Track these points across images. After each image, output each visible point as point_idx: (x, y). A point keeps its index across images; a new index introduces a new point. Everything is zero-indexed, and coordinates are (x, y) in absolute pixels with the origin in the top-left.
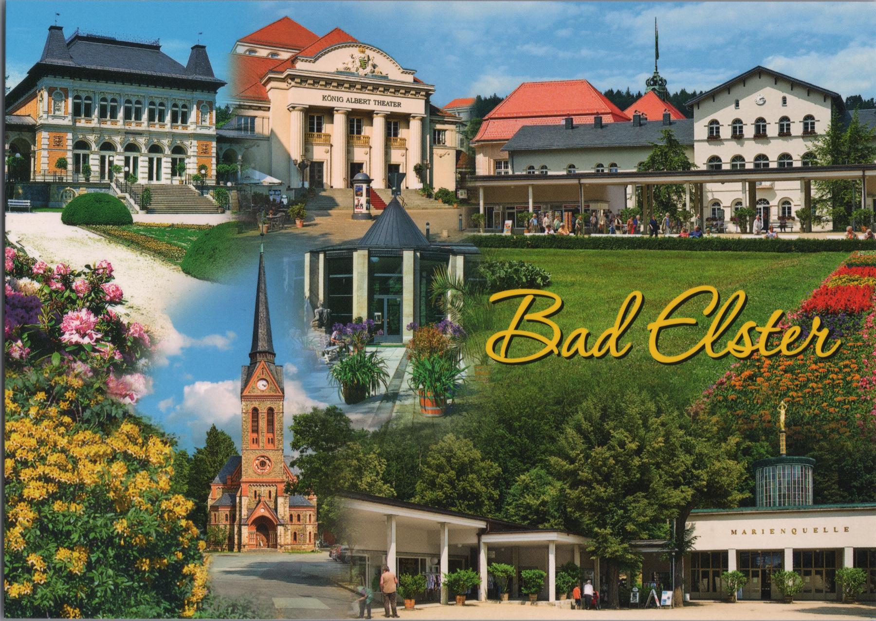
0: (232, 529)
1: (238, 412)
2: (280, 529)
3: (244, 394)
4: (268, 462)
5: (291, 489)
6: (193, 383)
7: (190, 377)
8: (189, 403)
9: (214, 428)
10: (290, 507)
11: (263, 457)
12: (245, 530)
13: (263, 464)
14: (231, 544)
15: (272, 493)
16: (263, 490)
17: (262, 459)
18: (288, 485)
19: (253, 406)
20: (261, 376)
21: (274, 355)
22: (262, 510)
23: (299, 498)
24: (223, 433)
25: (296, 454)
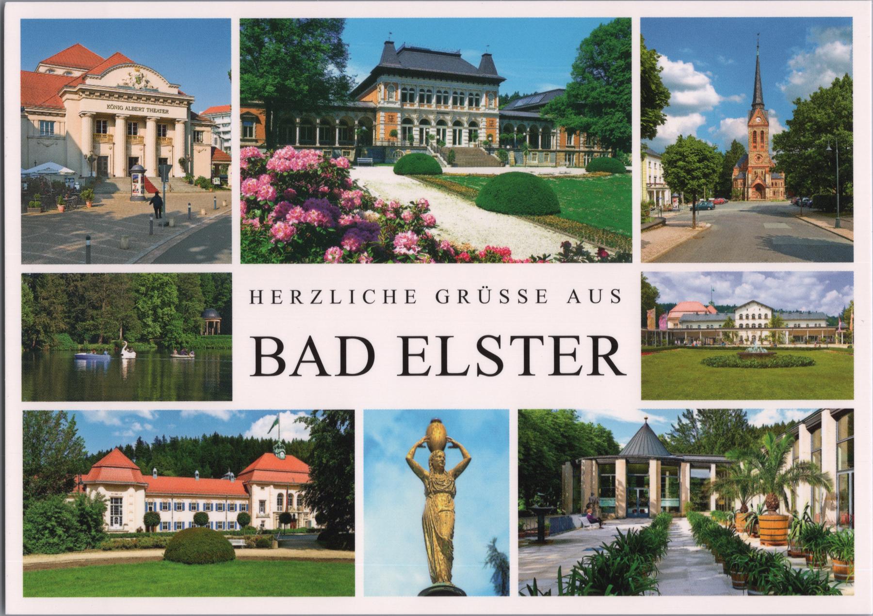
0: (744, 190)
1: (747, 133)
2: (767, 190)
3: (750, 124)
5: (772, 170)
6: (724, 119)
7: (723, 116)
8: (723, 129)
9: (735, 141)
12: (750, 190)
13: (759, 158)
14: (744, 197)
16: (759, 171)
18: (771, 168)
21: (763, 105)
23: (775, 174)
24: (739, 144)
25: (775, 153)
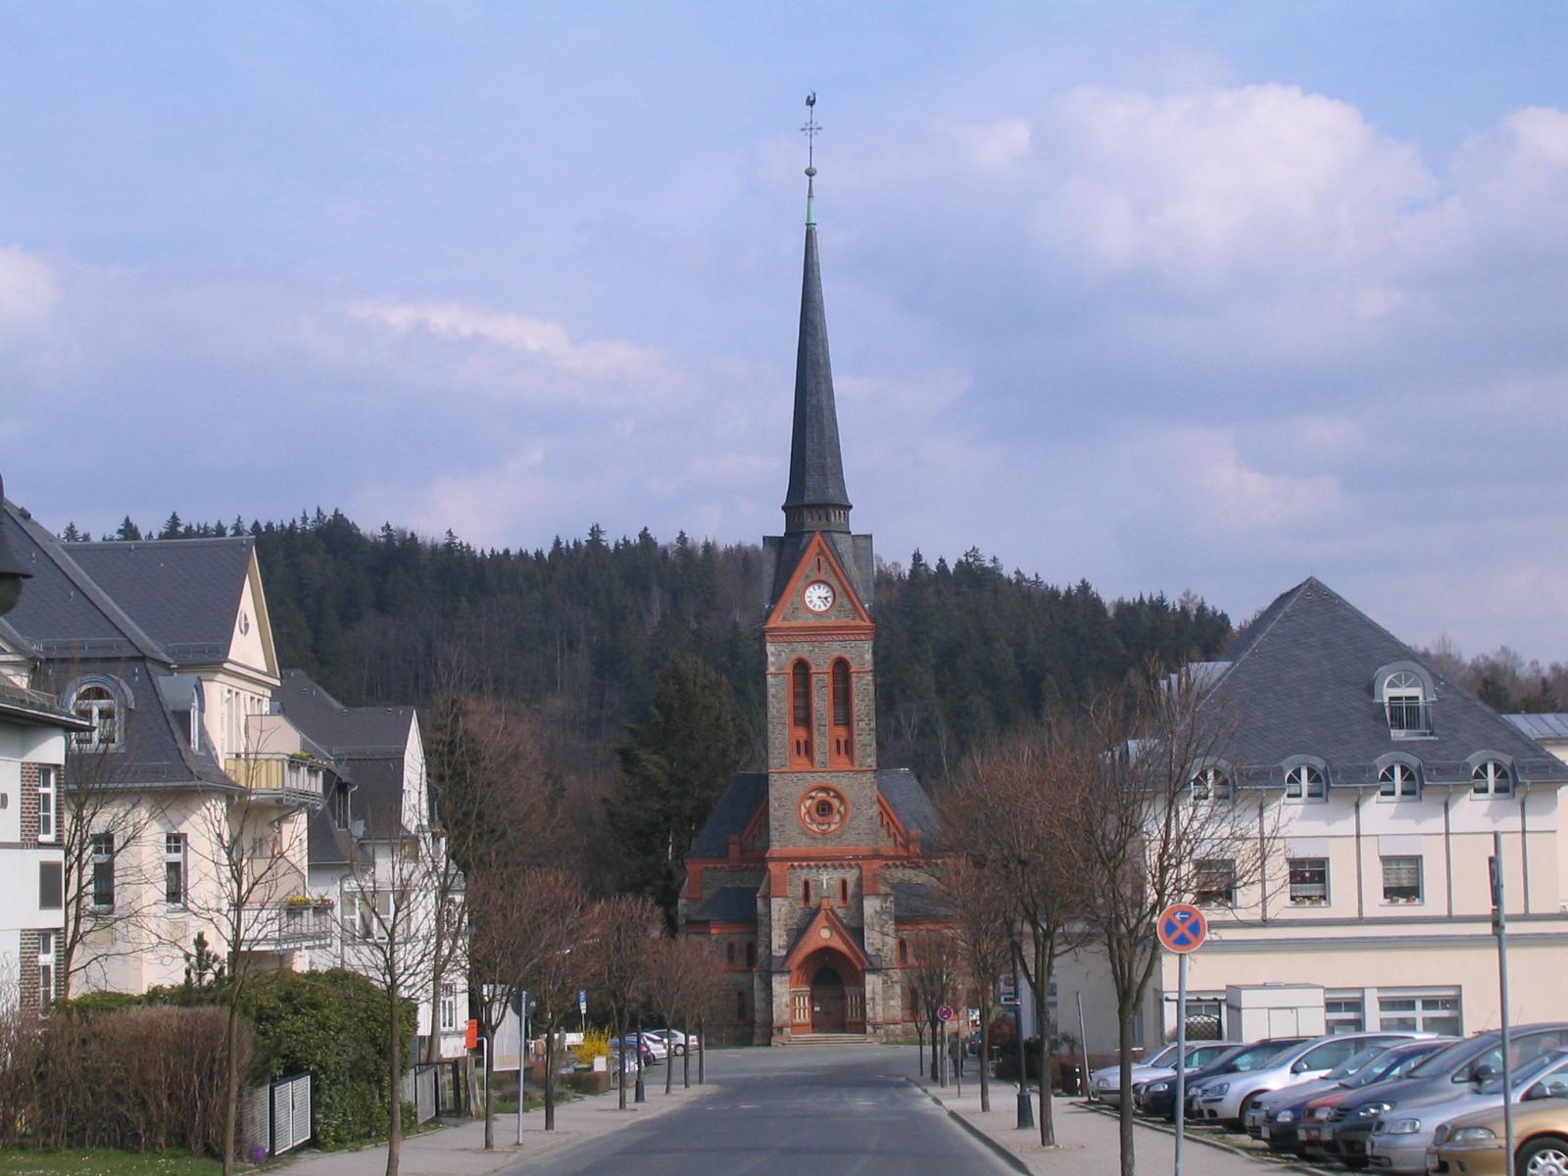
2: (872, 983)
4: (836, 803)
10: (899, 921)
12: (781, 987)
13: (824, 809)
16: (827, 879)
17: (822, 795)
19: (794, 656)
20: (815, 576)
22: (825, 934)
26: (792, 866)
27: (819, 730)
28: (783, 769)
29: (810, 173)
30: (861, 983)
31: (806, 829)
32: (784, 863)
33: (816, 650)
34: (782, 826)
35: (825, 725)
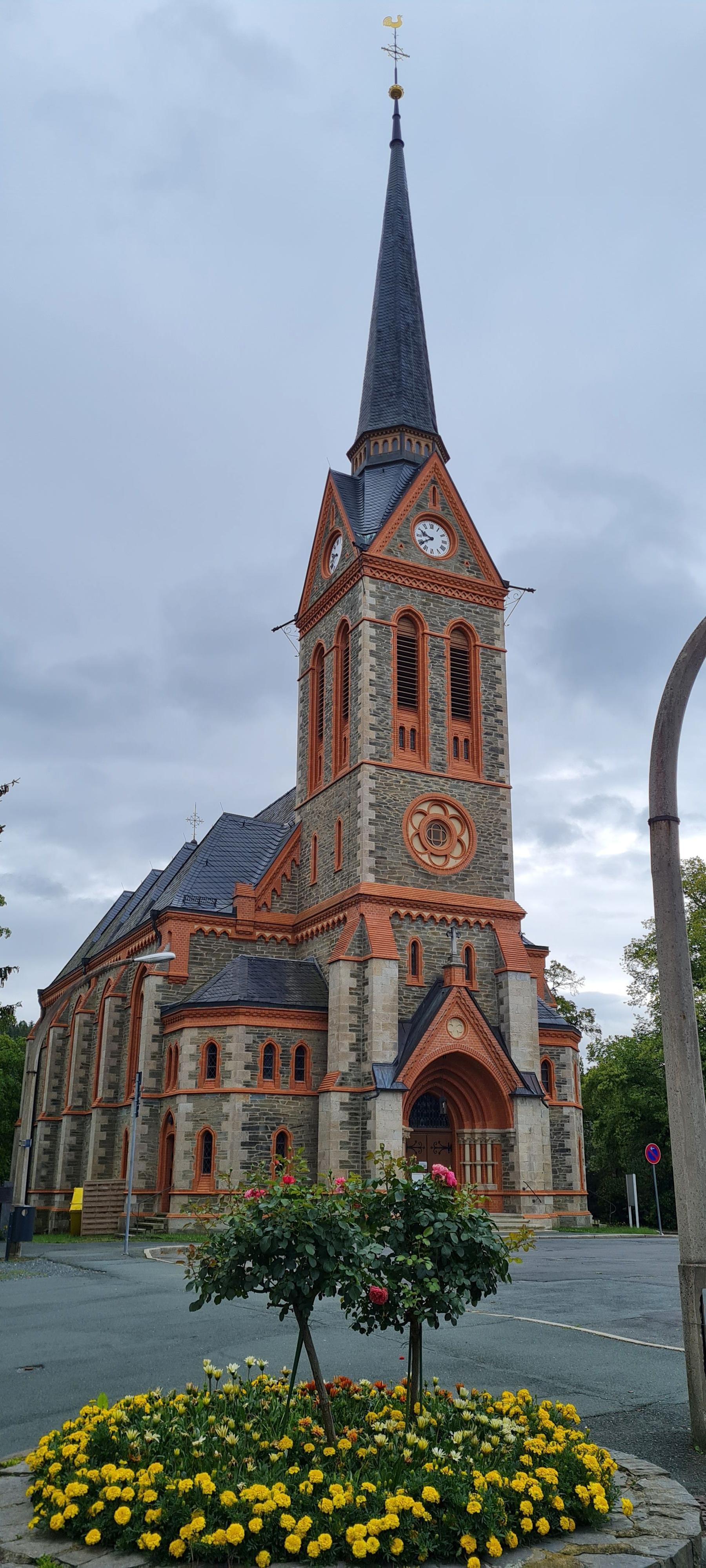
11: (439, 802)
15: (476, 957)
17: (436, 811)
20: (429, 508)
26: (396, 914)
27: (433, 715)
28: (384, 762)
29: (396, 94)
30: (505, 1120)
31: (418, 861)
32: (386, 908)
33: (432, 606)
34: (384, 849)
35: (442, 711)
